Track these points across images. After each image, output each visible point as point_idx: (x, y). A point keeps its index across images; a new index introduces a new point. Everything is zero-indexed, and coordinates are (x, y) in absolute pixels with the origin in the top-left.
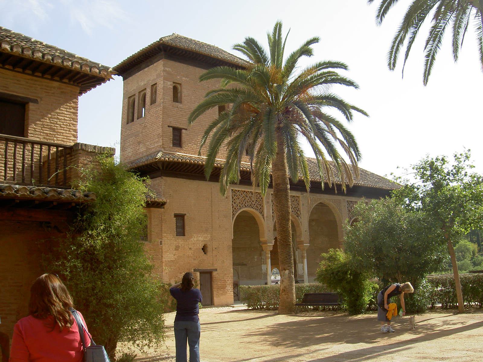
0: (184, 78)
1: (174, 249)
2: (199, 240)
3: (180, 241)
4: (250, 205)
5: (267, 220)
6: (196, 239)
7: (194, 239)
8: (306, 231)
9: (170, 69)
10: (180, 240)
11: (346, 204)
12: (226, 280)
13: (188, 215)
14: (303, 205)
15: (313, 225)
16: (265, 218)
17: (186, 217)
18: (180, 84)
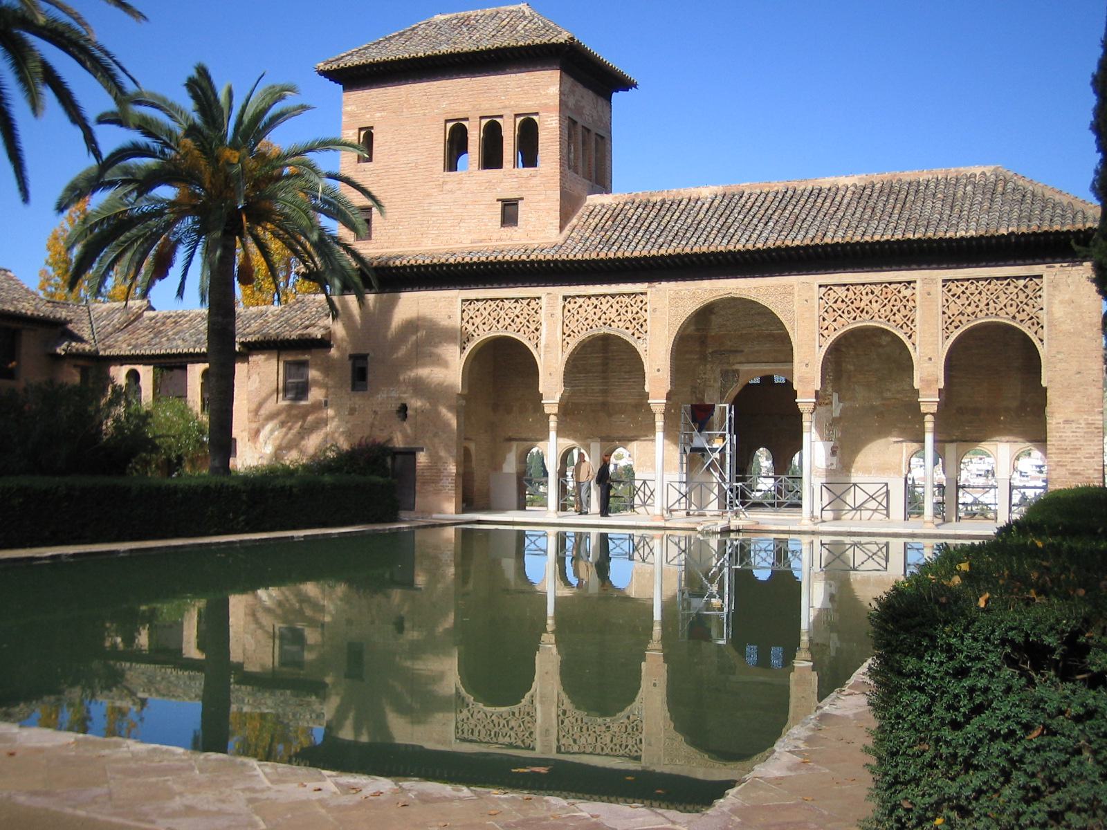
0: (378, 115)
1: (347, 413)
2: (391, 397)
3: (358, 400)
4: (510, 325)
5: (545, 351)
6: (385, 396)
7: (380, 397)
8: (659, 370)
9: (354, 108)
10: (357, 399)
11: (817, 292)
12: (442, 468)
13: (372, 355)
14: (655, 310)
15: (884, 343)
16: (543, 349)
17: (369, 358)
18: (372, 127)
